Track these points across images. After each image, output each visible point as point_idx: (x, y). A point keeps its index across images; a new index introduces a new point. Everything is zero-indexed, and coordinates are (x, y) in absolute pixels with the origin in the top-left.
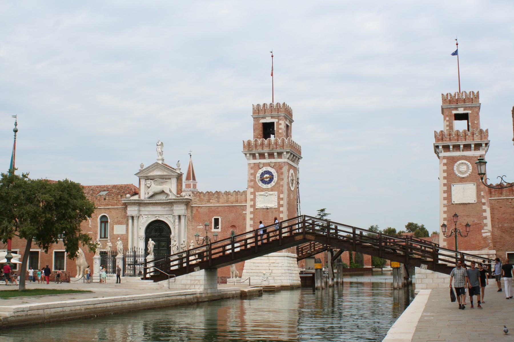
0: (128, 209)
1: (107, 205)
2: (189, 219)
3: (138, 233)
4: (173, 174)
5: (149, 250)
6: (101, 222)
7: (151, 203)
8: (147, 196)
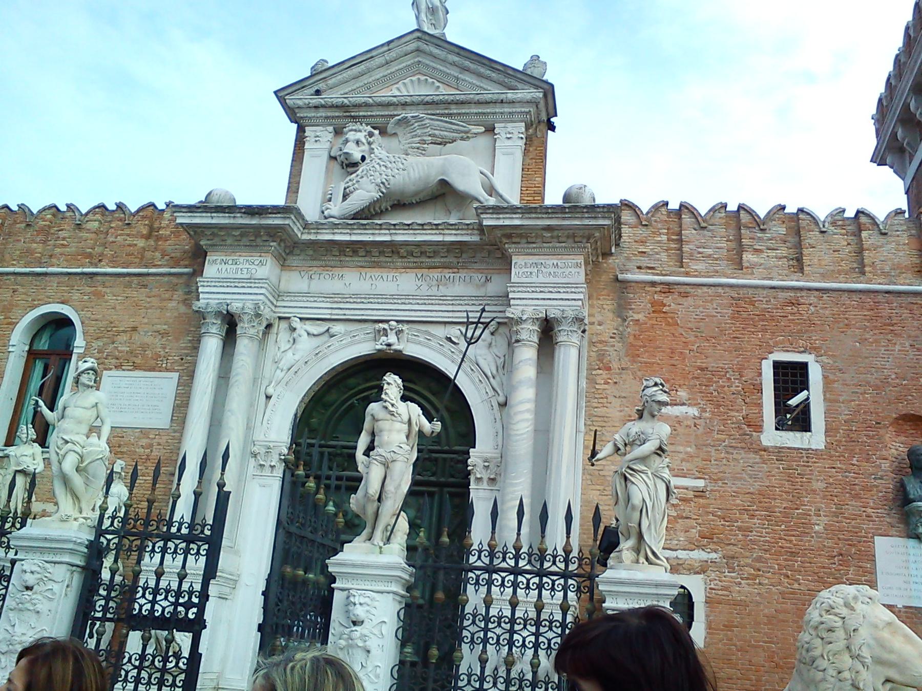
0: (210, 270)
2: (601, 356)
3: (249, 428)
4: (511, 95)
6: (32, 355)
7: (354, 248)
8: (336, 208)
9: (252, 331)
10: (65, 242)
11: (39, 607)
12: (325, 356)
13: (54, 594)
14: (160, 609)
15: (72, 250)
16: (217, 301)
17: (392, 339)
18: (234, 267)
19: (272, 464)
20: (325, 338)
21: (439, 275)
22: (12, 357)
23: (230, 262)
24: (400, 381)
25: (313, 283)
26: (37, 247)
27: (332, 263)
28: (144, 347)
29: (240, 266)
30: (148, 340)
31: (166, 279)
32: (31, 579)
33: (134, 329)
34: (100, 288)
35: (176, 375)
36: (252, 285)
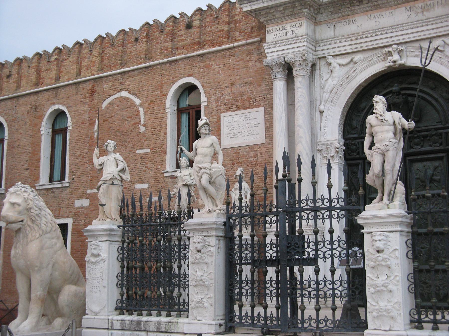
0: (270, 37)
1: (200, 45)
3: (313, 134)
5: (376, 168)
6: (180, 111)
9: (303, 72)
10: (183, 38)
11: (206, 260)
12: (354, 78)
13: (212, 253)
14: (269, 255)
15: (188, 42)
16: (277, 57)
17: (396, 57)
18: (285, 31)
19: (332, 155)
20: (351, 65)
21: (422, 4)
22: (169, 115)
23: (281, 29)
24: (384, 99)
25: (337, 29)
26: (169, 45)
27: (346, 13)
28: (241, 94)
29: (288, 30)
30: (242, 89)
31: (245, 48)
32: (199, 246)
33: (233, 84)
34: (208, 63)
35: (262, 109)
36: (297, 41)
